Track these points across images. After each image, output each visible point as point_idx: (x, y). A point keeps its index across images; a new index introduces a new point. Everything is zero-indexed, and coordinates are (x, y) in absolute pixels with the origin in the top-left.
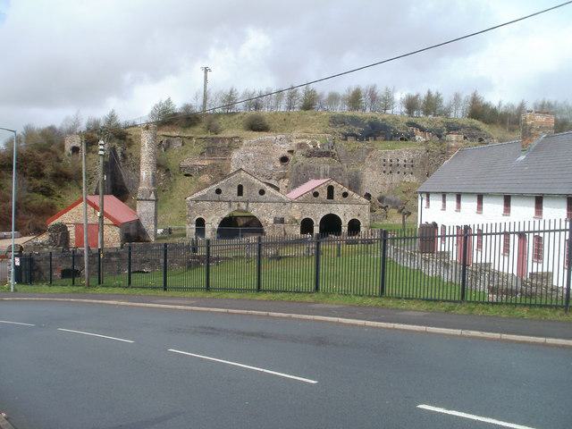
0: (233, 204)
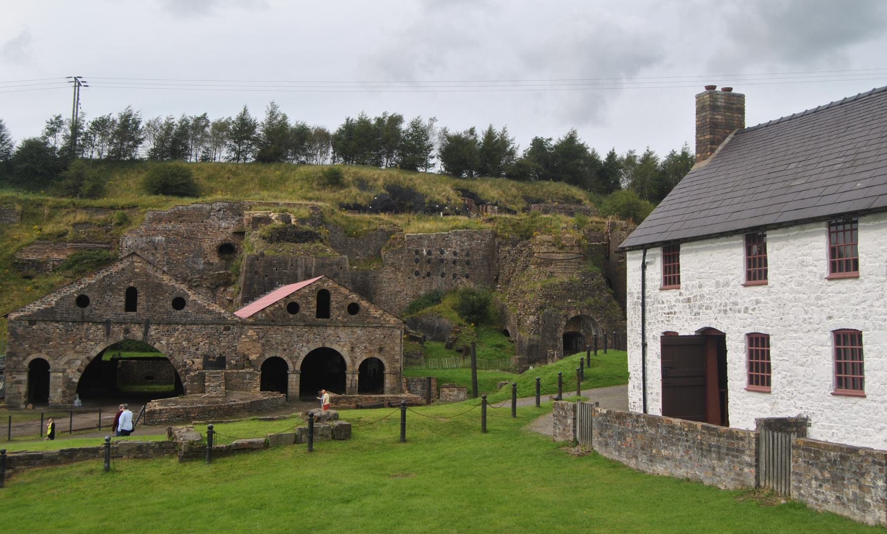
0: (115, 328)
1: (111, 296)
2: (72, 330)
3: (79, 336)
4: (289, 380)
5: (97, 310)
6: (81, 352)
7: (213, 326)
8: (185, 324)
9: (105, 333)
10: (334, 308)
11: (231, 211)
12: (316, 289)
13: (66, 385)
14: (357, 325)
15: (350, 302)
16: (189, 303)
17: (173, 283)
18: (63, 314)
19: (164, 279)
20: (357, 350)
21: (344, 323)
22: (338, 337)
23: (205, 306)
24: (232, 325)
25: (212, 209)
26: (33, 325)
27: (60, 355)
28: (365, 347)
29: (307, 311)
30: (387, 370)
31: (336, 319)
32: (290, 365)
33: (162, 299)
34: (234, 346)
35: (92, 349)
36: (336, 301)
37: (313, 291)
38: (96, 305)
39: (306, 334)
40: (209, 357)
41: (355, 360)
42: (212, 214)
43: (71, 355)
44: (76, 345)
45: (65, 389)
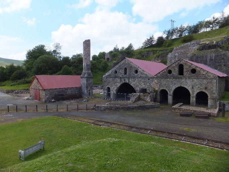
15: (192, 68)
20: (194, 88)
21: (189, 77)
28: (198, 87)
30: (209, 97)
32: (169, 92)
43: (114, 86)
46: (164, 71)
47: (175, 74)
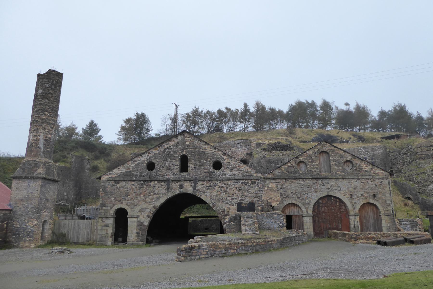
1: (170, 162)
2: (144, 187)
3: (148, 191)
4: (304, 222)
5: (161, 172)
6: (150, 203)
7: (243, 181)
8: (223, 180)
9: (166, 188)
10: (333, 165)
11: (244, 144)
12: (317, 151)
13: (139, 228)
14: (353, 177)
16: (225, 165)
17: (213, 151)
18: (138, 175)
19: (206, 148)
21: (342, 176)
22: (339, 187)
23: (236, 167)
24: (256, 179)
25: (235, 143)
26: (117, 184)
27: (135, 205)
28: (362, 195)
29: (313, 168)
31: (336, 173)
33: (206, 163)
34: (259, 196)
35: (157, 200)
36: (334, 159)
37: (316, 152)
38: (160, 169)
39: (314, 185)
40: (242, 203)
41: (355, 205)
42: (235, 145)
43: (142, 205)
44: (146, 197)
45: (138, 231)
46: (289, 164)
47: (313, 170)
